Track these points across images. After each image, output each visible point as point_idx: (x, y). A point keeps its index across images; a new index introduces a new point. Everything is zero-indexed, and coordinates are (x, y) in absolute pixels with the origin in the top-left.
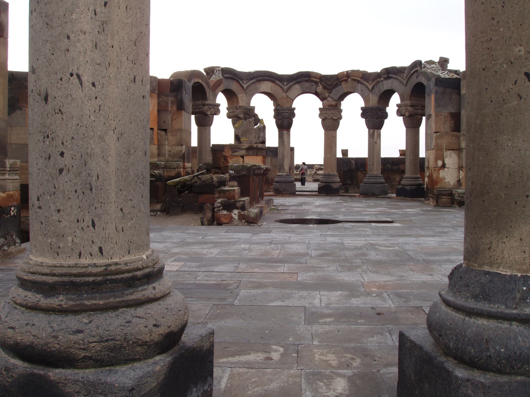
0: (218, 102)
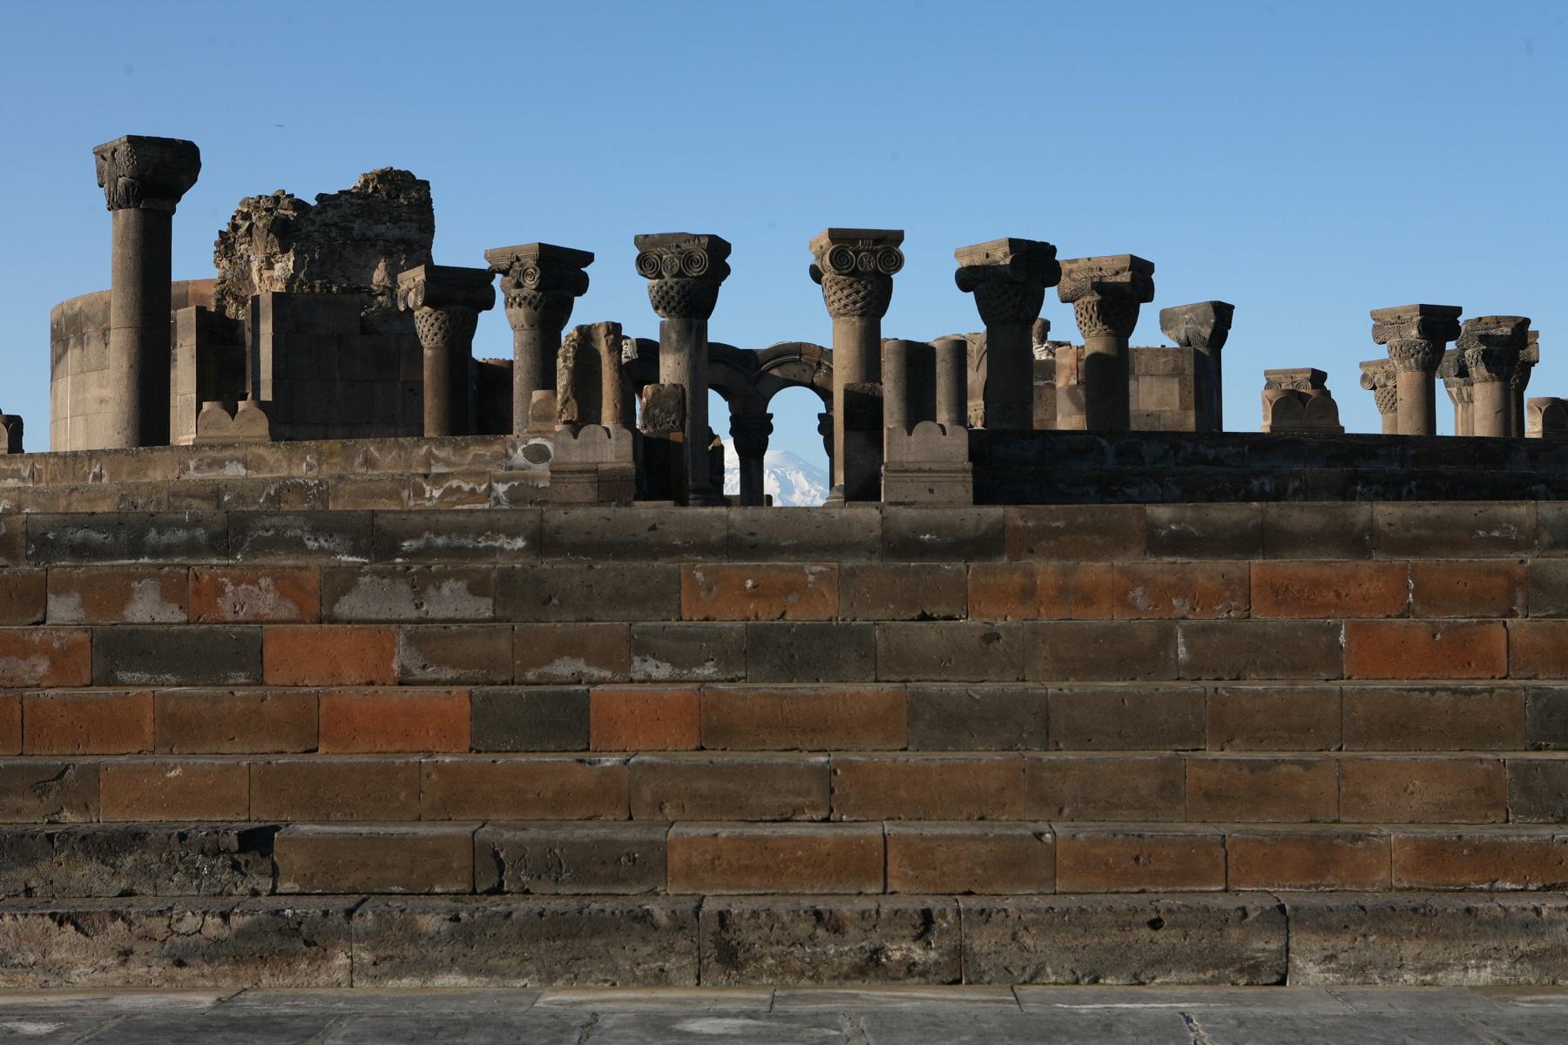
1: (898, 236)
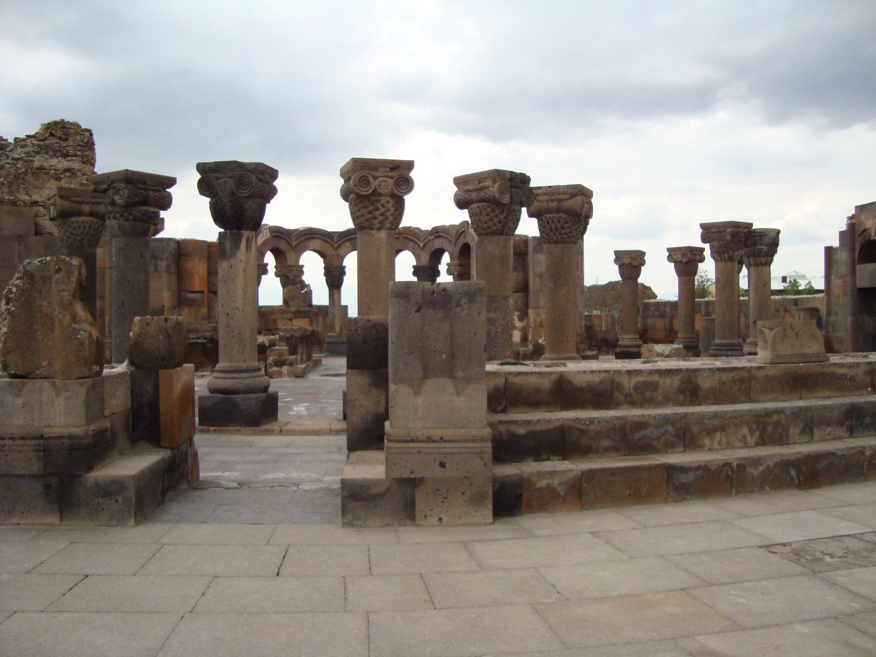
0: (266, 261)
1: (409, 165)
